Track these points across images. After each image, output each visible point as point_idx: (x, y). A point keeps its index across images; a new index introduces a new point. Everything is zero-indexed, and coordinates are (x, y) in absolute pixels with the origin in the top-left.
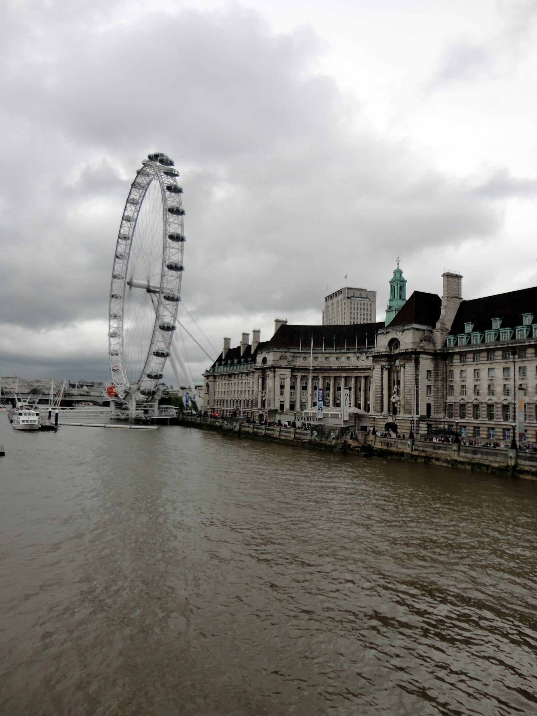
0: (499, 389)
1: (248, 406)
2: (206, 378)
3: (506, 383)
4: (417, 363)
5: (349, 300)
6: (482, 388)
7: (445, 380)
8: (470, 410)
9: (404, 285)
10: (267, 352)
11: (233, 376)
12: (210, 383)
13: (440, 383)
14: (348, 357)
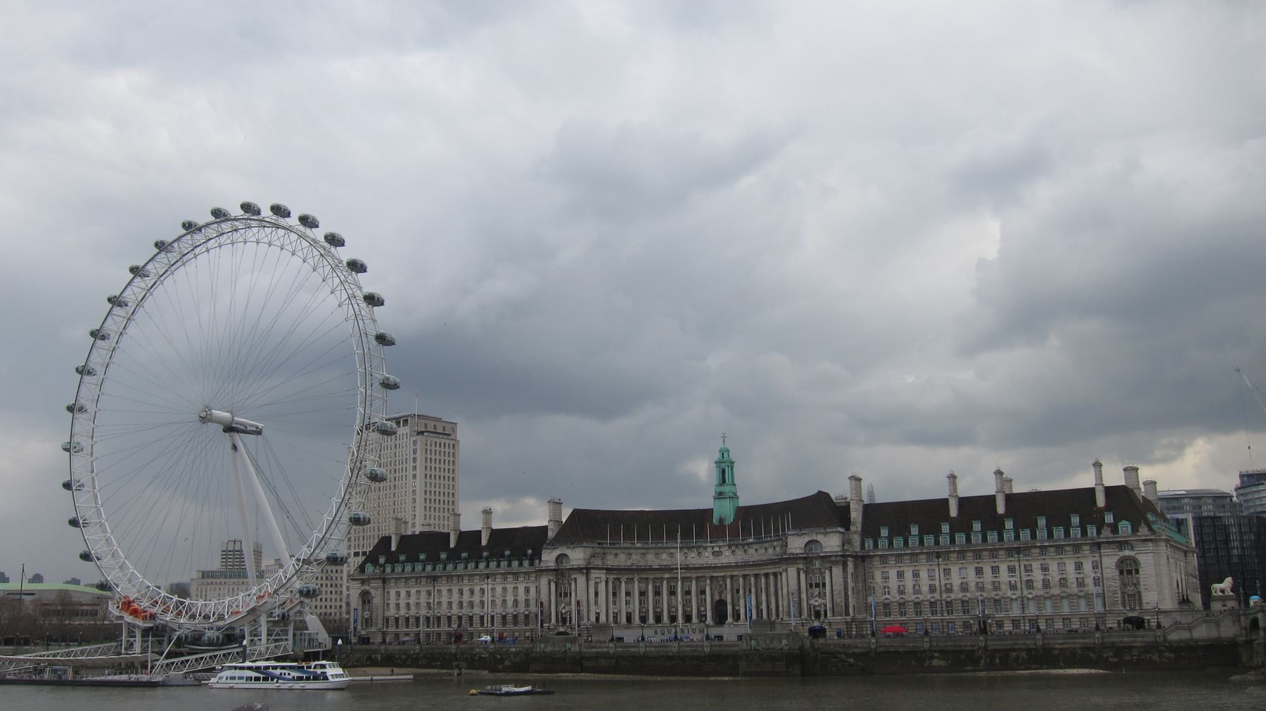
0: (925, 589)
1: (493, 624)
2: (359, 582)
3: (932, 583)
4: (845, 565)
5: (424, 438)
6: (906, 587)
7: (865, 581)
8: (895, 609)
9: (732, 467)
10: (568, 547)
11: (444, 579)
12: (371, 590)
13: (861, 585)
14: (671, 553)
